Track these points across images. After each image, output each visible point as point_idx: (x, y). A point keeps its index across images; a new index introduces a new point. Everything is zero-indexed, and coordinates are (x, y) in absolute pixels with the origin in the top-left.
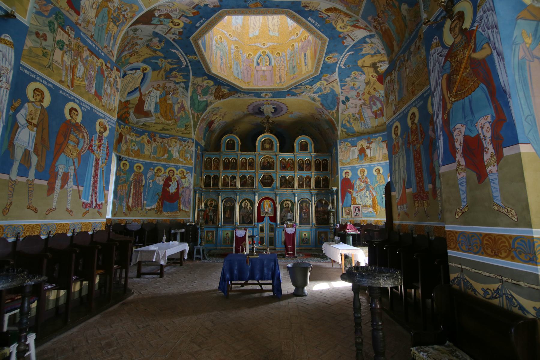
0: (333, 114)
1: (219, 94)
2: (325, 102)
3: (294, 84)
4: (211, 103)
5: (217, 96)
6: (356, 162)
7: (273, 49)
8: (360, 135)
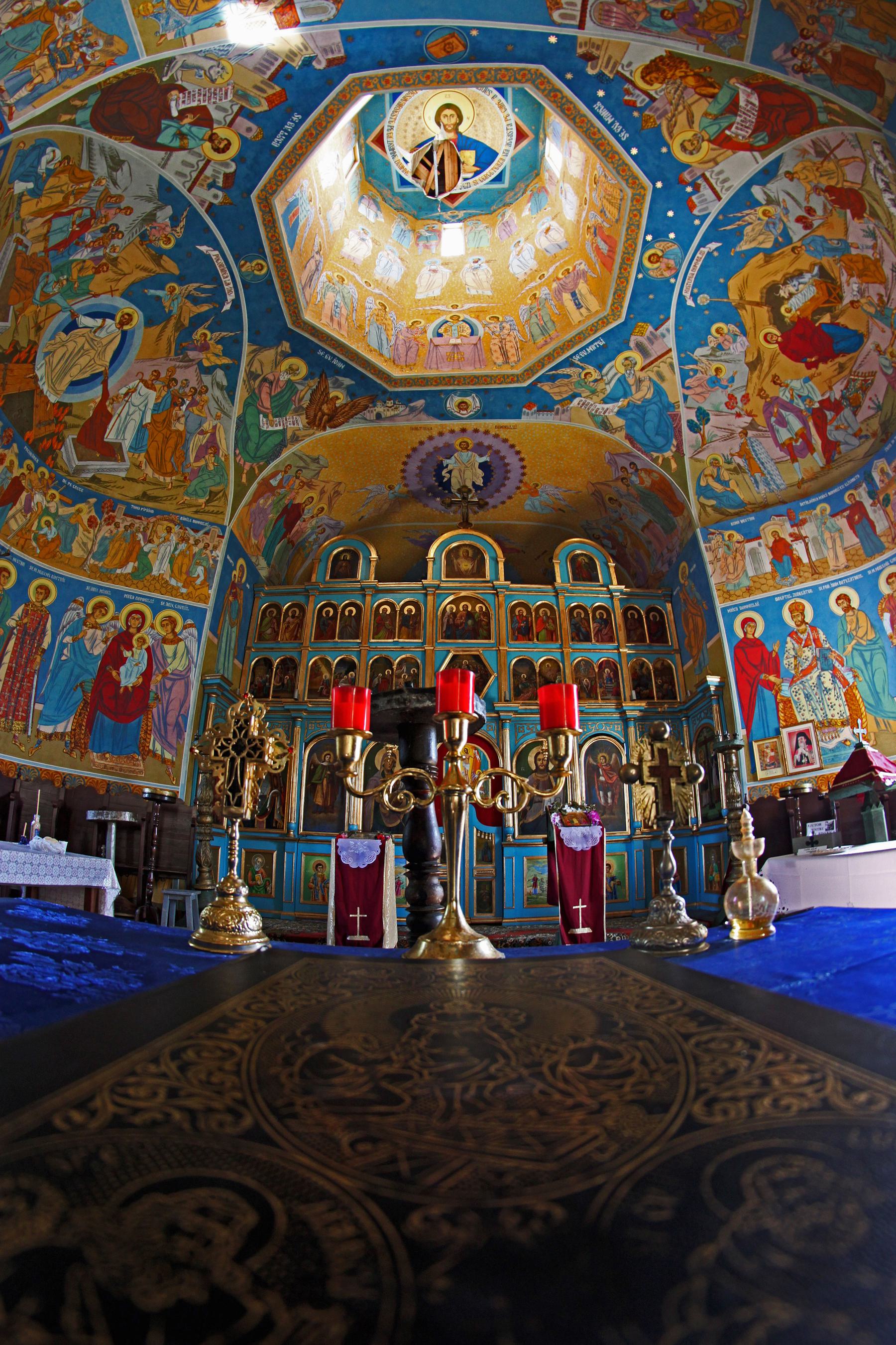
0: (666, 463)
1: (320, 409)
2: (637, 429)
3: (550, 357)
4: (296, 439)
5: (315, 416)
6: (771, 582)
7: (478, 313)
8: (763, 508)
